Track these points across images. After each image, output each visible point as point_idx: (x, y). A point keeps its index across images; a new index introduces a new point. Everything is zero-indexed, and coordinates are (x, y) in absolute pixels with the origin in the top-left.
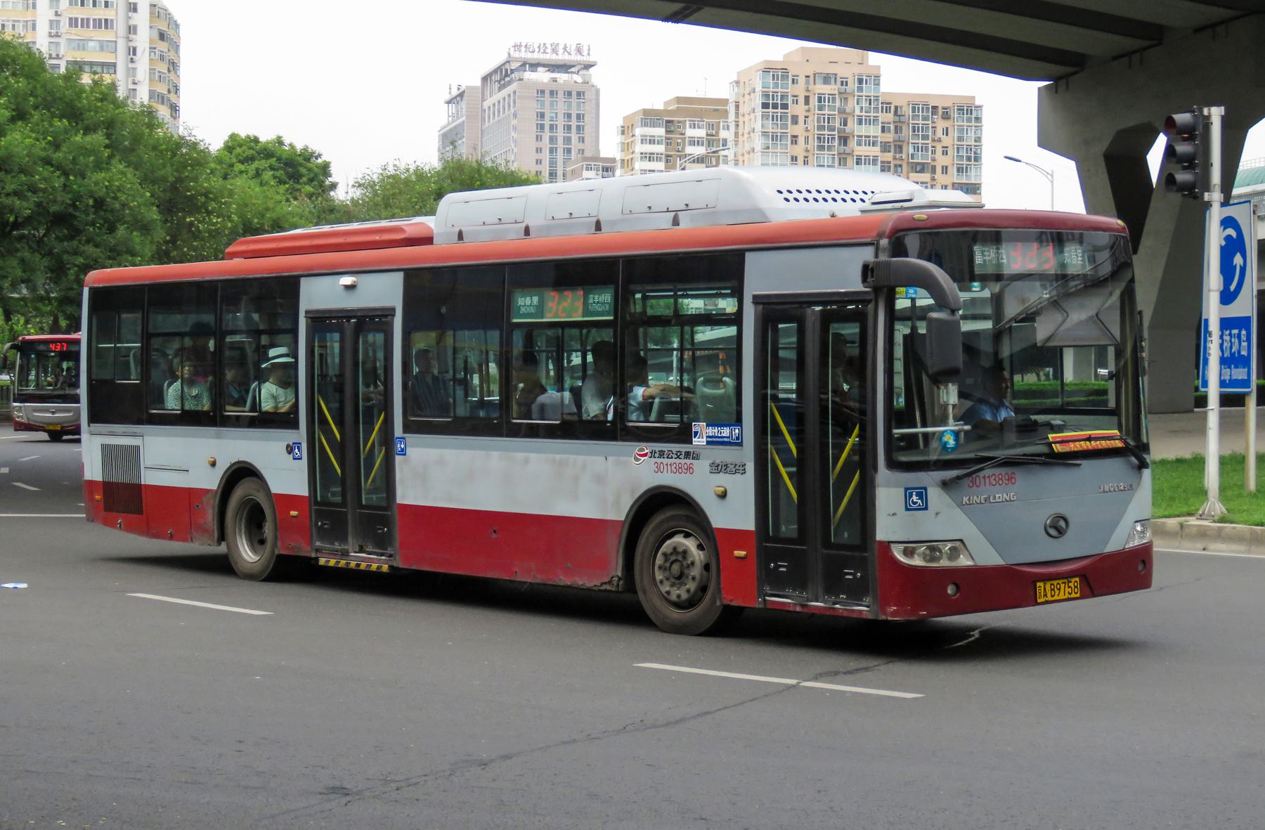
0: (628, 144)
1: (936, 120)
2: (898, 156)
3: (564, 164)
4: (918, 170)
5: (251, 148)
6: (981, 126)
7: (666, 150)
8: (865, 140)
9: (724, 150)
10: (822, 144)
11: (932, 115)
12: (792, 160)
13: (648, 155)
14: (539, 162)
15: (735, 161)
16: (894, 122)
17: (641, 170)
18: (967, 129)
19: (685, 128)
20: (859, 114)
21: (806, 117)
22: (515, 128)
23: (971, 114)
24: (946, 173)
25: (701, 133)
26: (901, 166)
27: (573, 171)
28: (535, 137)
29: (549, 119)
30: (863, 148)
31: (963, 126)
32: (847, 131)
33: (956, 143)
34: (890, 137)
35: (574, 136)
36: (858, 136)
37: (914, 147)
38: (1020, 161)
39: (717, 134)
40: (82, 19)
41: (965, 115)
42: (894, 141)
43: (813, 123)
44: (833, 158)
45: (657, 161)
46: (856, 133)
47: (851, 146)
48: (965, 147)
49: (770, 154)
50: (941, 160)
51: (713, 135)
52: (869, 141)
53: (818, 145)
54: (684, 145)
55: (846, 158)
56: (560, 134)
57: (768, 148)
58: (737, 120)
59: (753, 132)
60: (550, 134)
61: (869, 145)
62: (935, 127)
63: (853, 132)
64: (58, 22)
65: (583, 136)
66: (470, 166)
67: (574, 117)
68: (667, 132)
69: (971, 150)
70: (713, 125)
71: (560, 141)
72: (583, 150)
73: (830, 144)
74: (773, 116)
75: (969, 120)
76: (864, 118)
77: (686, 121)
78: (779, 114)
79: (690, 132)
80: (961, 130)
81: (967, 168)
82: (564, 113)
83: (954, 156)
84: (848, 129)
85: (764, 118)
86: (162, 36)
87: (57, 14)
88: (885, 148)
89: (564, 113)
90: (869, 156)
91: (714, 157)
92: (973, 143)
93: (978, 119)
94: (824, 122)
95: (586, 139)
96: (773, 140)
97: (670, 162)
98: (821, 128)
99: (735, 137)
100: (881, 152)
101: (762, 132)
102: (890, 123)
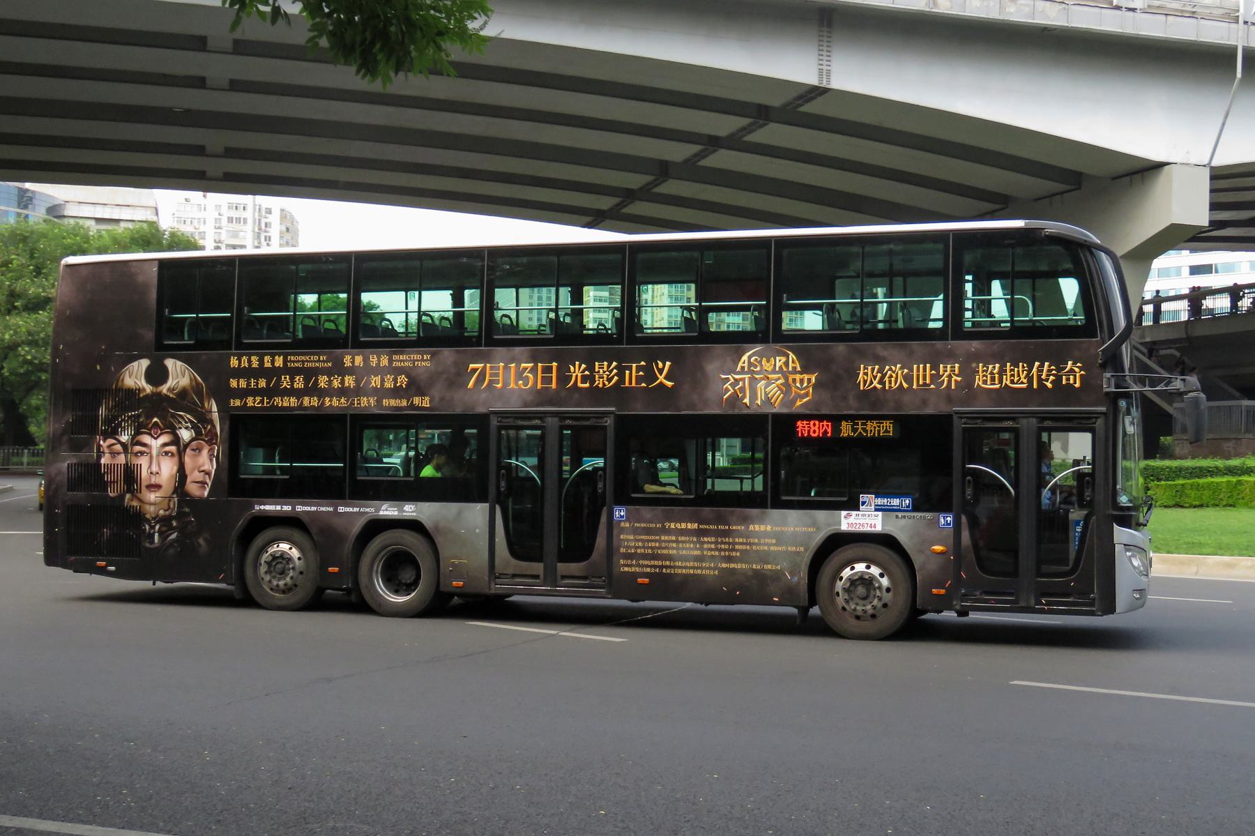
5: (334, 302)
40: (236, 218)
64: (220, 219)
68: (610, 294)
86: (288, 230)
87: (220, 215)
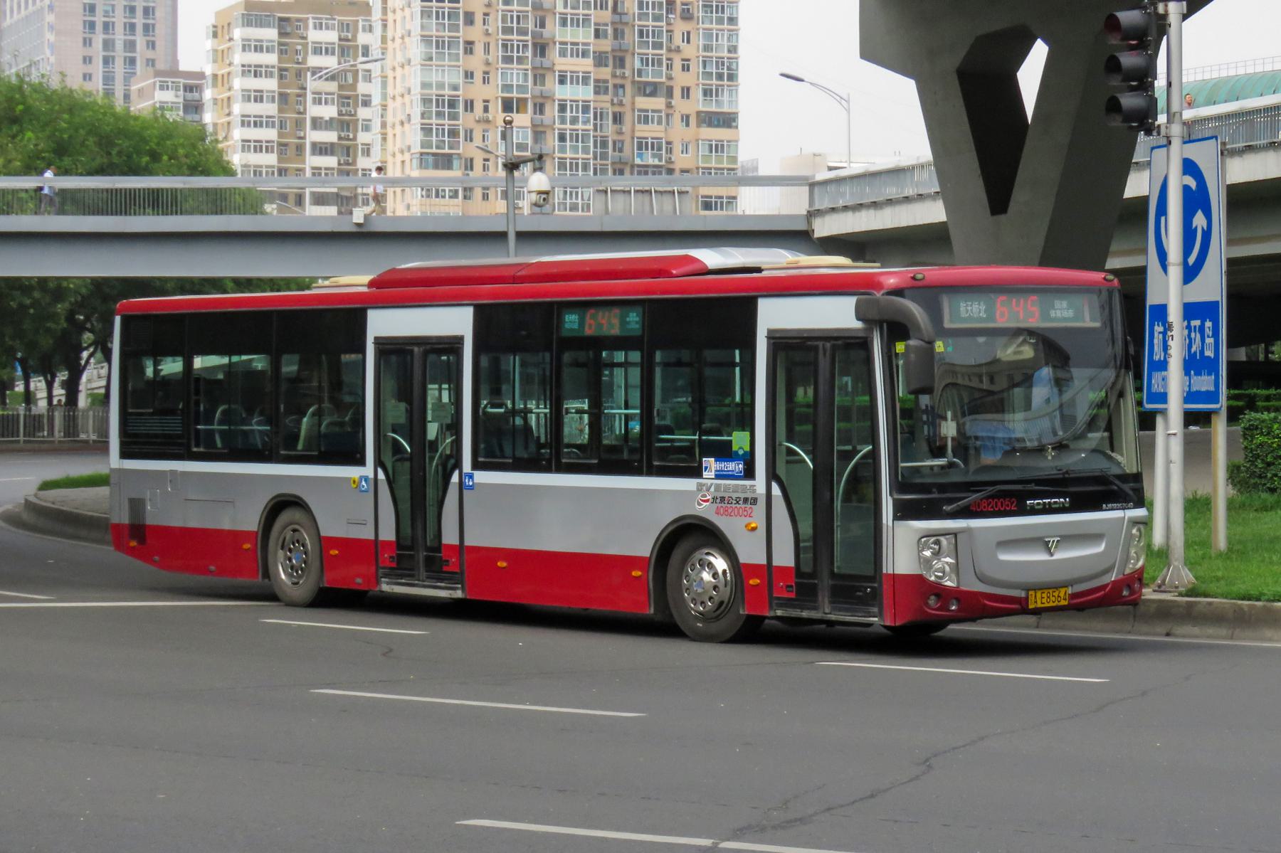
0: (223, 51)
1: (672, 21)
2: (618, 72)
3: (125, 78)
4: (648, 92)
6: (737, 30)
7: (280, 61)
8: (572, 49)
9: (376, 61)
10: (509, 54)
11: (667, 13)
12: (466, 76)
13: (253, 69)
14: (87, 77)
15: (382, 77)
16: (613, 23)
17: (243, 90)
18: (717, 35)
19: (306, 28)
20: (563, 10)
21: (486, 14)
22: (51, 27)
23: (723, 12)
24: (688, 97)
25: (331, 36)
26: (623, 86)
27: (140, 91)
28: (81, 40)
29: (102, 13)
30: (569, 60)
31: (712, 29)
32: (544, 36)
33: (702, 53)
34: (606, 45)
35: (140, 40)
36: (561, 43)
37: (642, 59)
38: (802, 80)
39: (355, 37)
41: (714, 15)
42: (613, 50)
43: (496, 23)
44: (526, 75)
45: (266, 77)
46: (558, 38)
47: (551, 58)
48: (714, 59)
49: (434, 68)
50: (681, 79)
51: (348, 40)
52: (578, 49)
53: (503, 56)
54: (306, 53)
55: (543, 76)
56: (119, 37)
57: (431, 59)
58: (384, 17)
59: (409, 35)
60: (106, 36)
61: (578, 56)
62: (671, 31)
63: (554, 37)
65: (153, 39)
66: (9, 82)
67: (139, 12)
68: (281, 34)
69: (723, 64)
70: (348, 25)
71: (119, 45)
72: (153, 61)
73: (521, 54)
74: (437, 13)
75: (720, 21)
76: (569, 17)
77: (308, 19)
78: (446, 10)
79: (314, 35)
80: (708, 35)
81: (717, 90)
82: (125, 6)
83: (698, 73)
84: (546, 33)
85: (425, 16)
88: (600, 60)
89: (125, 6)
90: (578, 72)
91: (350, 71)
92: (726, 54)
93: (732, 20)
94: (512, 22)
95: (157, 44)
96: (437, 47)
97: (286, 78)
98: (508, 30)
99: (382, 43)
100: (595, 66)
101: (422, 36)
102: (607, 25)
